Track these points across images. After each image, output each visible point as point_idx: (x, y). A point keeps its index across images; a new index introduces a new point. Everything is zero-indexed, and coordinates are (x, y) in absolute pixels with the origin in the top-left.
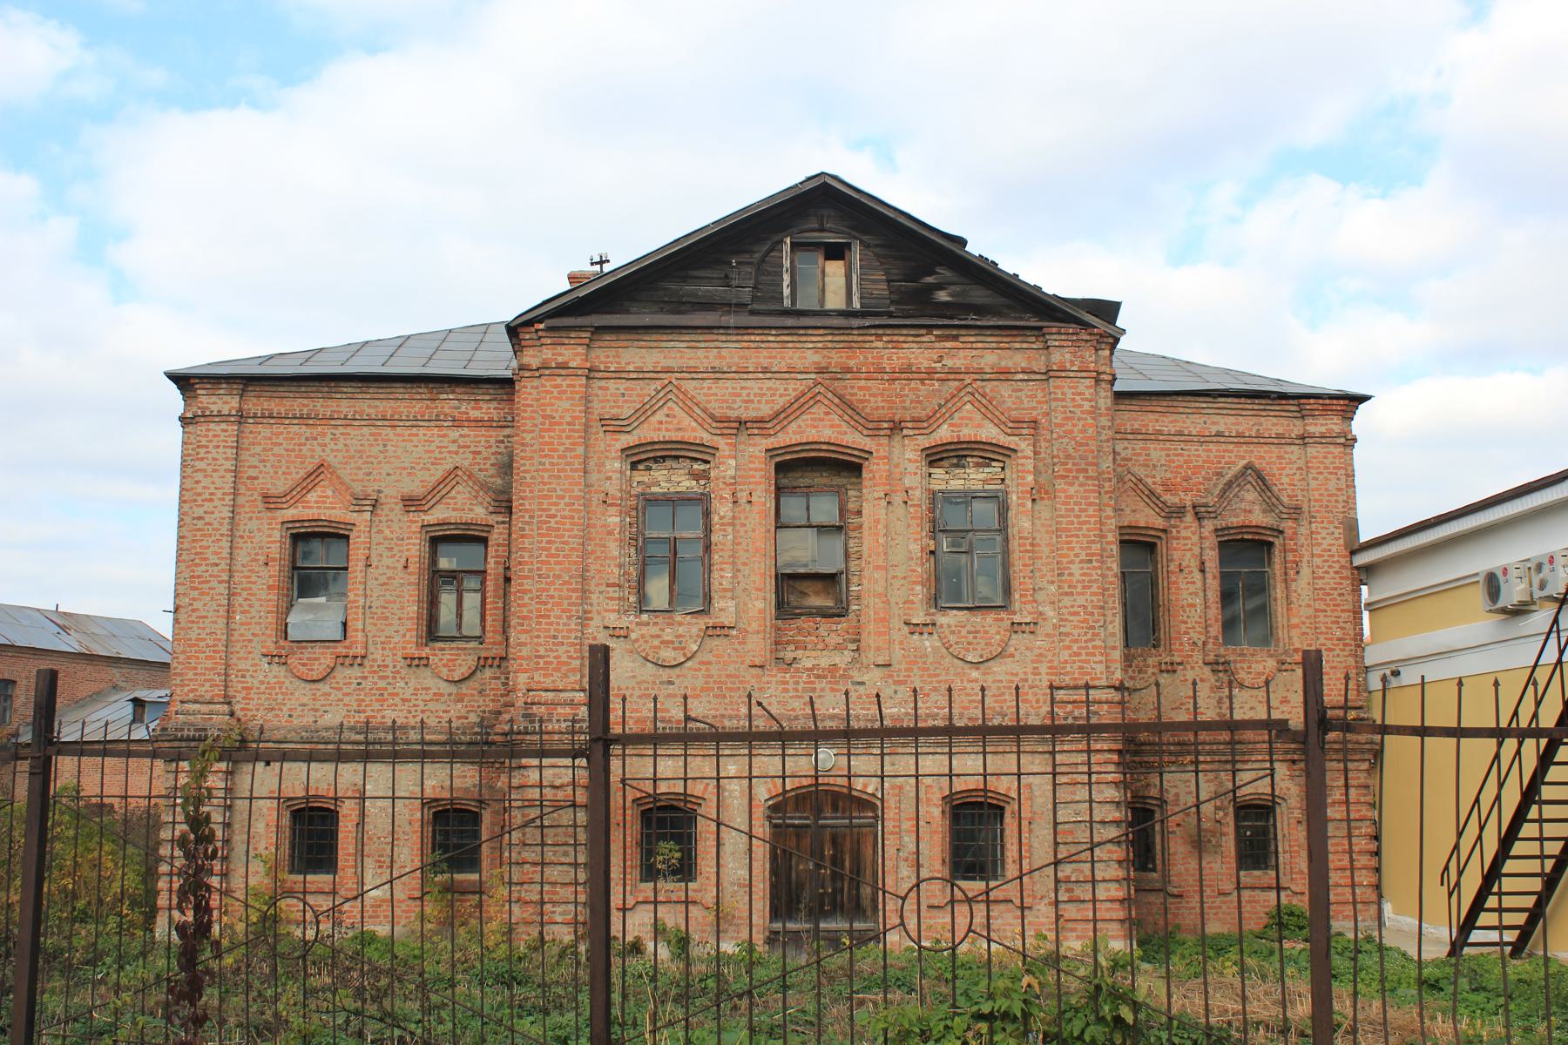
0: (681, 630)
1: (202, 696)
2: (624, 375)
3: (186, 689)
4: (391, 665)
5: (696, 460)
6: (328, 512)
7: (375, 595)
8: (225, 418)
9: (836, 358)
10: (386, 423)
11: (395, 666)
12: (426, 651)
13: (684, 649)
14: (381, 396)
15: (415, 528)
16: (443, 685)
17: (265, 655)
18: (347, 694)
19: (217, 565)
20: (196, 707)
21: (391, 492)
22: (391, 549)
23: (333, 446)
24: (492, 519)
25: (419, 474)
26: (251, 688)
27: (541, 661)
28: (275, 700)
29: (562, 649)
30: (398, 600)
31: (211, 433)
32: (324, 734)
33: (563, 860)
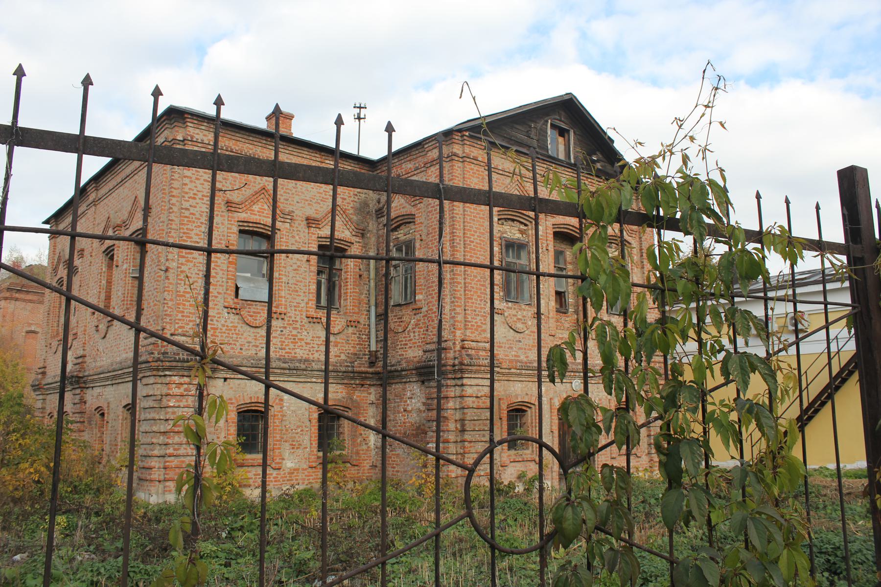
0: (525, 313)
1: (187, 331)
3: (177, 326)
4: (299, 321)
7: (291, 276)
11: (302, 322)
13: (525, 323)
14: (295, 153)
15: (314, 237)
24: (354, 239)
25: (315, 205)
26: (217, 329)
27: (470, 324)
28: (232, 338)
29: (478, 318)
30: (303, 280)
33: (483, 439)
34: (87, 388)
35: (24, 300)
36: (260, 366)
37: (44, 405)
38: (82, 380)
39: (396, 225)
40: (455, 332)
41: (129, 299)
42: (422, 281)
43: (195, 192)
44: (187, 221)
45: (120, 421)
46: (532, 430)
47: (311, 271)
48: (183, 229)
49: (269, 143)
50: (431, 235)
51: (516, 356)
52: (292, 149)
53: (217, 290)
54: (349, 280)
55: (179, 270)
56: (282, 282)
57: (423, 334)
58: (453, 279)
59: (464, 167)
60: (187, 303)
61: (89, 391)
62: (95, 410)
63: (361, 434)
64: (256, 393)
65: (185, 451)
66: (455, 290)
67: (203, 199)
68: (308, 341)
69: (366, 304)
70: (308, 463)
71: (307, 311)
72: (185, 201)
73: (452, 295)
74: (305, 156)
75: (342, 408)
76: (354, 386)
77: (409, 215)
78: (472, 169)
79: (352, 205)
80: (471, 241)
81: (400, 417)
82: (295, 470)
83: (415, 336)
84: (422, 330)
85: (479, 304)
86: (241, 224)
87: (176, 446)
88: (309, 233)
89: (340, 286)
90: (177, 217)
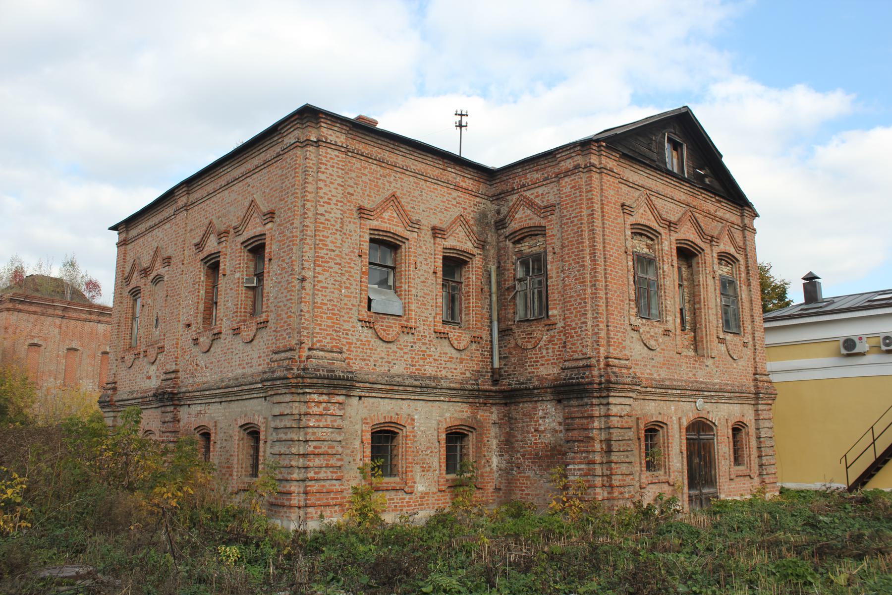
0: (656, 330)
1: (325, 346)
2: (628, 183)
3: (315, 339)
5: (648, 237)
6: (395, 228)
7: (419, 288)
8: (338, 148)
9: (690, 200)
10: (423, 177)
11: (430, 337)
12: (447, 329)
14: (419, 159)
15: (440, 248)
16: (454, 351)
17: (360, 320)
18: (406, 353)
19: (334, 251)
20: (322, 353)
21: (429, 220)
22: (426, 260)
23: (402, 185)
24: (476, 251)
25: (439, 214)
28: (366, 353)
29: (620, 334)
31: (329, 156)
32: (397, 379)
34: (182, 405)
35: (27, 312)
36: (394, 383)
37: (115, 423)
38: (176, 397)
39: (520, 237)
40: (599, 349)
41: (243, 310)
42: (557, 296)
43: (330, 196)
44: (323, 228)
45: (236, 442)
46: (664, 451)
47: (437, 284)
48: (319, 236)
49: (396, 147)
50: (567, 248)
51: (650, 374)
52: (418, 155)
53: (352, 302)
54: (471, 294)
55: (316, 279)
56: (411, 295)
57: (558, 351)
58: (595, 293)
59: (601, 179)
60: (325, 316)
61: (181, 409)
62: (195, 429)
63: (485, 456)
64: (389, 412)
65: (325, 475)
66: (598, 306)
67: (337, 205)
68: (436, 357)
69: (488, 319)
70: (437, 487)
71: (435, 325)
72: (320, 205)
73: (594, 310)
74: (429, 163)
75: (467, 428)
76: (478, 405)
77: (537, 227)
78: (609, 181)
79: (472, 216)
80: (610, 255)
81: (531, 438)
82: (426, 493)
83: (550, 353)
84: (557, 347)
85: (620, 320)
86: (372, 232)
87: (316, 470)
88: (435, 244)
89: (461, 300)
90: (311, 223)
